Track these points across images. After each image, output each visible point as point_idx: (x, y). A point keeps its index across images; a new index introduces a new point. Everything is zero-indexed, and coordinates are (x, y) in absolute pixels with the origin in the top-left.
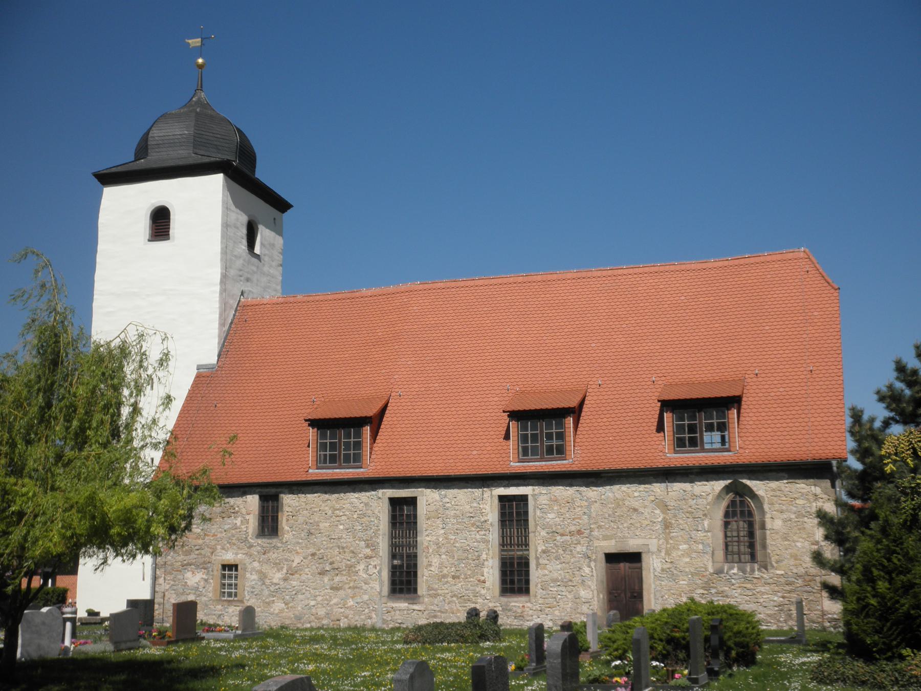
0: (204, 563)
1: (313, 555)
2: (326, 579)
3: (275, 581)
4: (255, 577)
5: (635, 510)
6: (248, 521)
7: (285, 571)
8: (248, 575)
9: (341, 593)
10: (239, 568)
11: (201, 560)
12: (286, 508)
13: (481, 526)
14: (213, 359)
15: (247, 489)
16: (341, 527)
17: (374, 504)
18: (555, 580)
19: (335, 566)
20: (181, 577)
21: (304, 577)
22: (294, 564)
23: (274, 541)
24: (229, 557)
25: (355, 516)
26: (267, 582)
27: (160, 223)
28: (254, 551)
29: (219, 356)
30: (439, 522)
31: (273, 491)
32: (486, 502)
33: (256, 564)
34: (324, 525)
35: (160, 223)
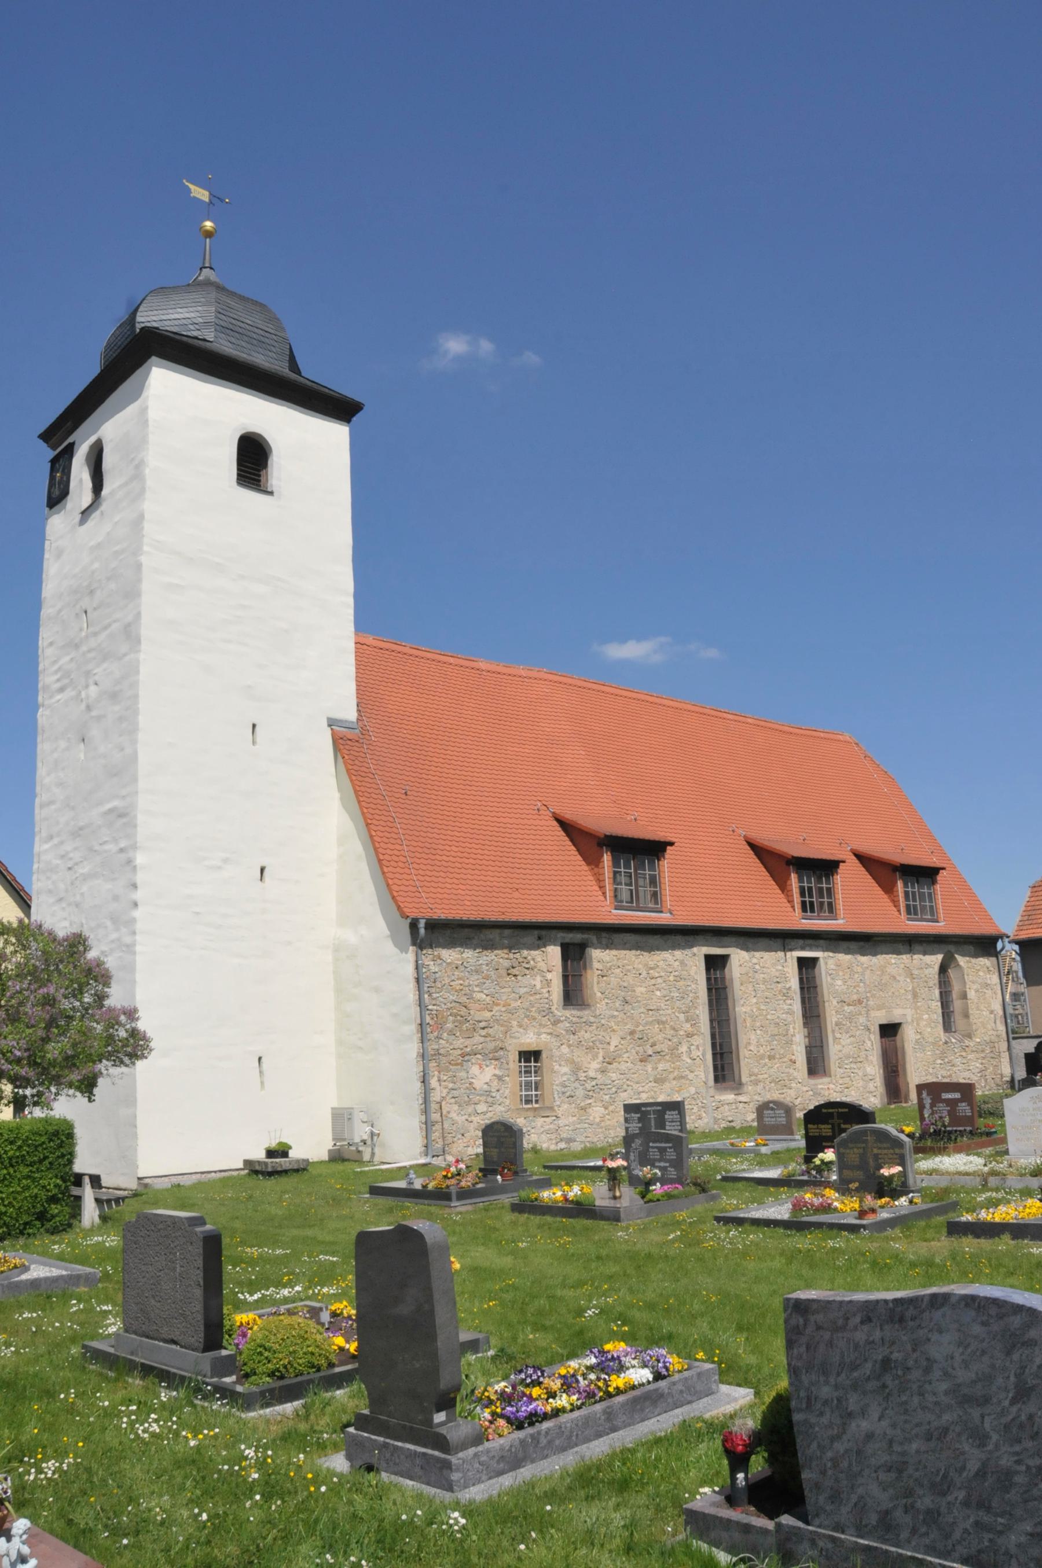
0: (496, 1050)
1: (632, 1033)
2: (649, 1068)
3: (592, 1074)
4: (565, 1069)
5: (894, 978)
6: (549, 983)
7: (601, 1058)
8: (556, 1067)
9: (667, 1085)
10: (544, 1055)
11: (491, 1046)
12: (596, 965)
13: (786, 994)
14: (350, 713)
15: (543, 933)
16: (658, 993)
17: (689, 962)
18: (848, 1057)
19: (658, 1048)
20: (463, 1074)
21: (623, 1066)
22: (612, 1048)
23: (586, 1013)
24: (530, 1040)
25: (672, 978)
26: (582, 1075)
27: (253, 458)
28: (561, 1028)
29: (359, 711)
30: (750, 987)
31: (577, 937)
32: (782, 965)
33: (565, 1049)
34: (640, 990)
35: (253, 458)
